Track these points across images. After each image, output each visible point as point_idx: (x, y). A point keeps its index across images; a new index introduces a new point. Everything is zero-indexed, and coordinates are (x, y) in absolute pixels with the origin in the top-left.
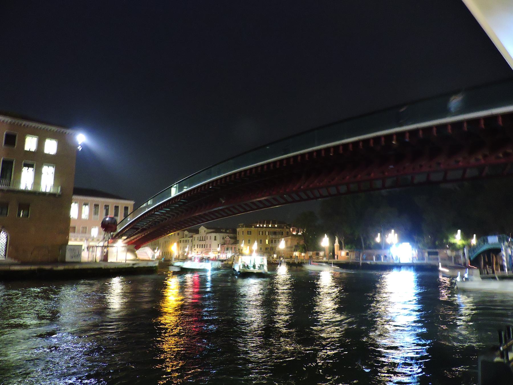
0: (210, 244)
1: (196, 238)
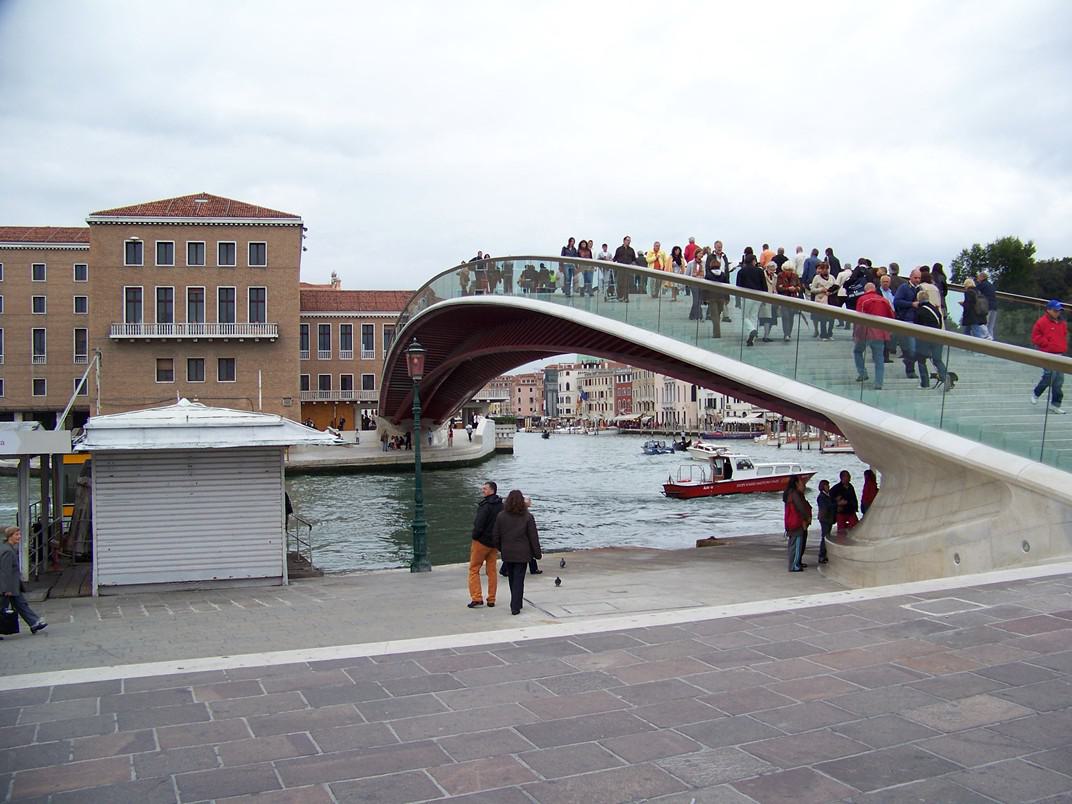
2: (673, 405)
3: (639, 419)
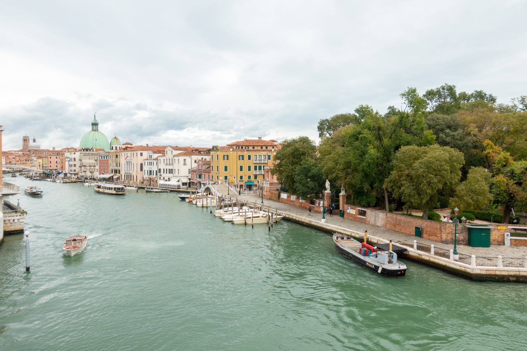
0: (178, 170)
1: (162, 161)
2: (130, 172)
3: (112, 176)
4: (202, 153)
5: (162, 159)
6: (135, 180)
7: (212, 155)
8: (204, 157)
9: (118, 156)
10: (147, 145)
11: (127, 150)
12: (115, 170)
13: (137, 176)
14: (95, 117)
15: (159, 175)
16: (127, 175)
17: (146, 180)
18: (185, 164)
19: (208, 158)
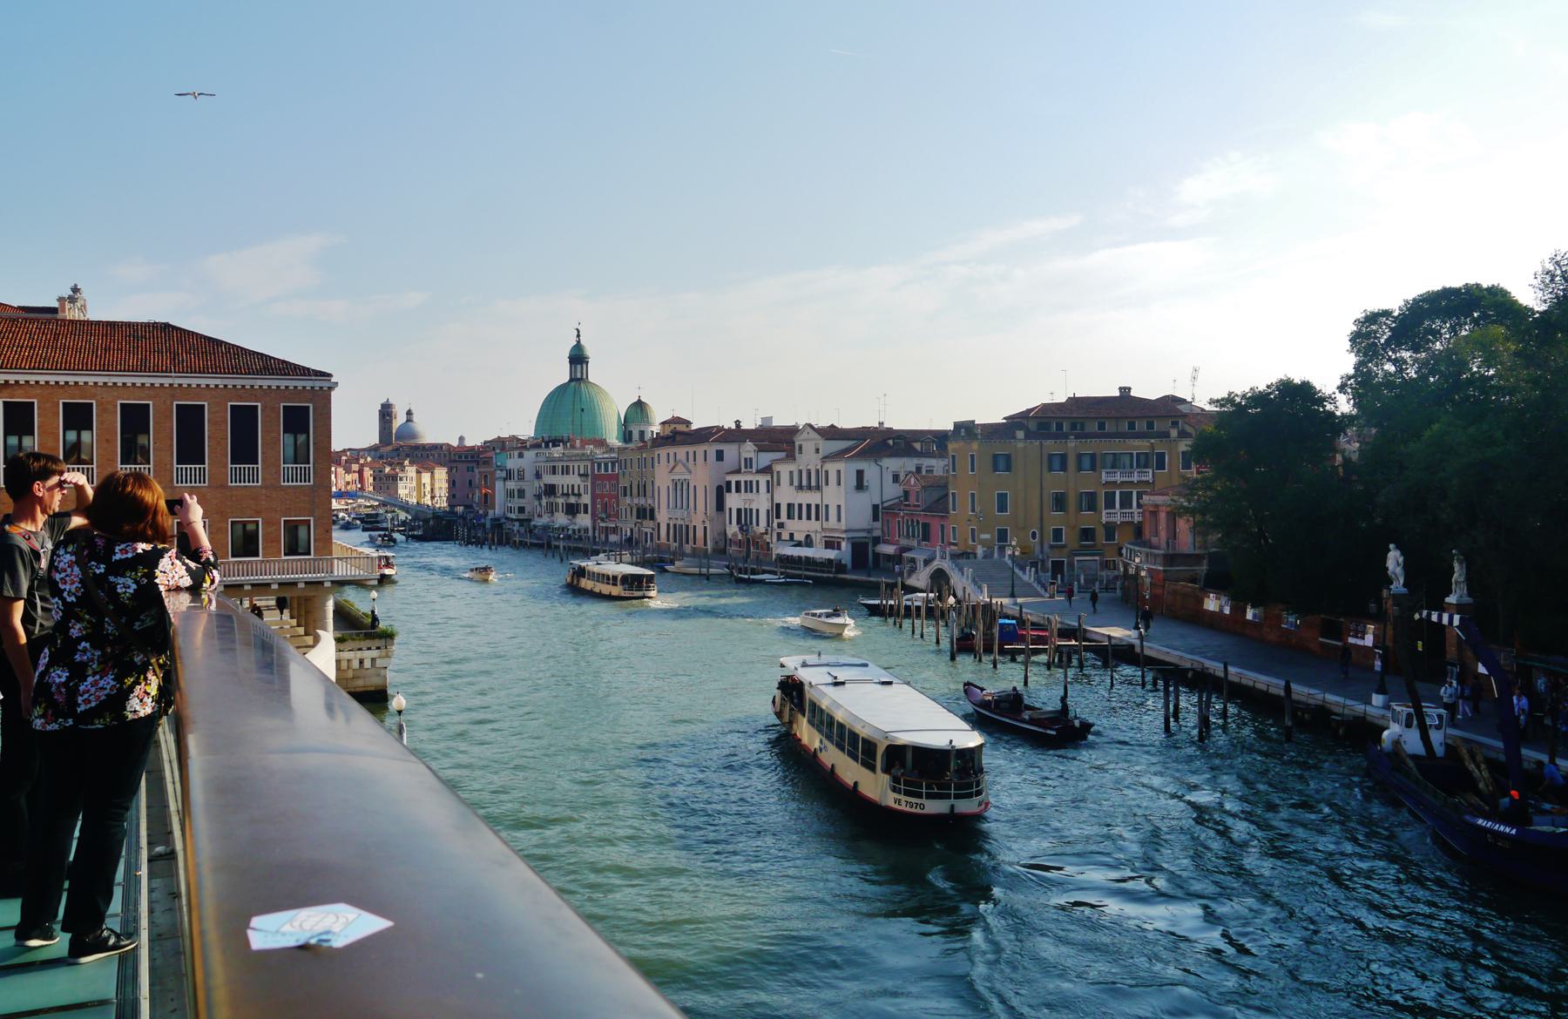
1: (785, 478)
4: (917, 446)
5: (784, 469)
6: (700, 543)
7: (953, 457)
8: (926, 462)
9: (649, 462)
10: (738, 423)
11: (674, 440)
12: (638, 510)
13: (705, 528)
14: (578, 336)
15: (775, 525)
16: (675, 525)
17: (735, 543)
18: (860, 486)
19: (938, 466)
